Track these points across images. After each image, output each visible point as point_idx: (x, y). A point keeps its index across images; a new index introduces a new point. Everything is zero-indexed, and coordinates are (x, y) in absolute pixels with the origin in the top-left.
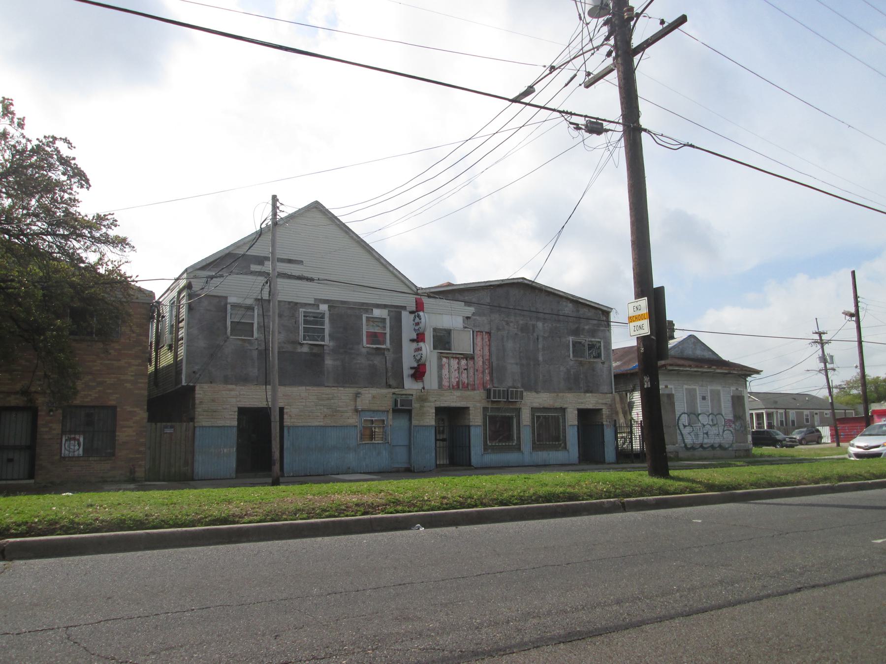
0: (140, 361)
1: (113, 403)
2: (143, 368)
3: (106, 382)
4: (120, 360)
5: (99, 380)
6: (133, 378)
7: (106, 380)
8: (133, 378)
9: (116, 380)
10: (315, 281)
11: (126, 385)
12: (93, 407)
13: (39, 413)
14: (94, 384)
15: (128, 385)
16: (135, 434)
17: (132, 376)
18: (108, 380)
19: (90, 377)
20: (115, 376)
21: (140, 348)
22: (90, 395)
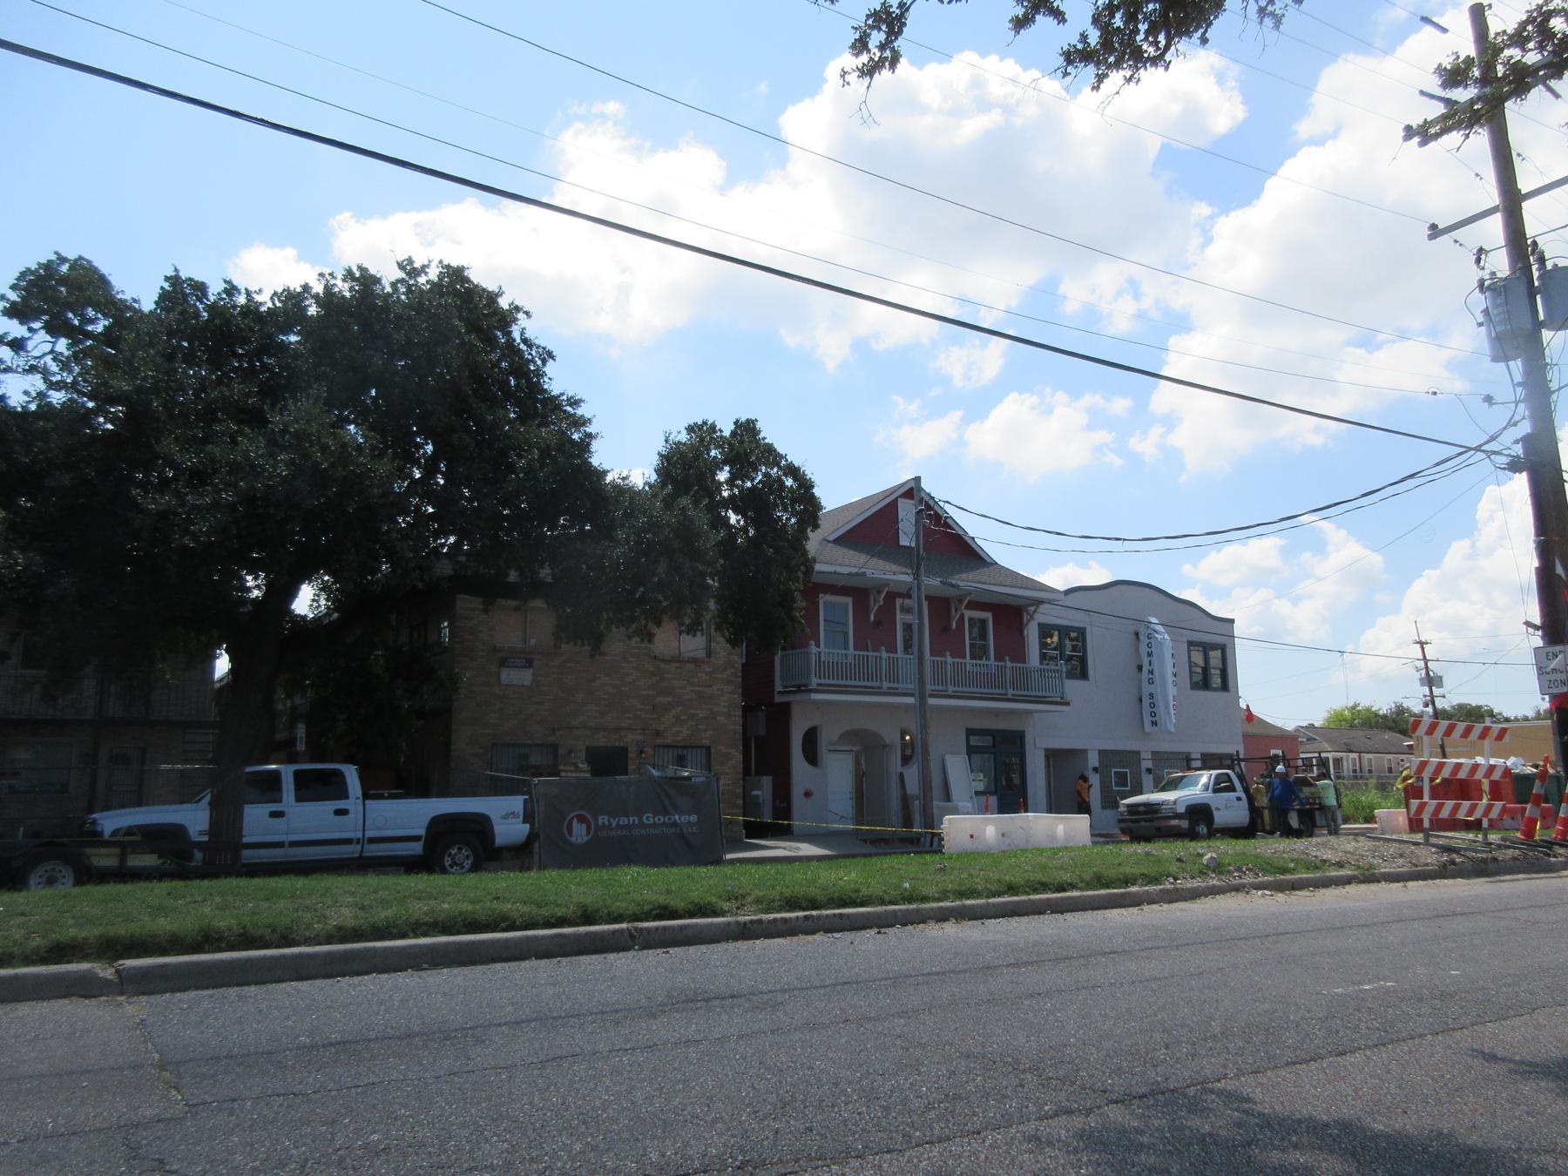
1: (705, 742)
6: (726, 710)
7: (699, 712)
8: (726, 710)
12: (687, 747)
15: (721, 719)
16: (730, 782)
17: (725, 707)
18: (699, 712)
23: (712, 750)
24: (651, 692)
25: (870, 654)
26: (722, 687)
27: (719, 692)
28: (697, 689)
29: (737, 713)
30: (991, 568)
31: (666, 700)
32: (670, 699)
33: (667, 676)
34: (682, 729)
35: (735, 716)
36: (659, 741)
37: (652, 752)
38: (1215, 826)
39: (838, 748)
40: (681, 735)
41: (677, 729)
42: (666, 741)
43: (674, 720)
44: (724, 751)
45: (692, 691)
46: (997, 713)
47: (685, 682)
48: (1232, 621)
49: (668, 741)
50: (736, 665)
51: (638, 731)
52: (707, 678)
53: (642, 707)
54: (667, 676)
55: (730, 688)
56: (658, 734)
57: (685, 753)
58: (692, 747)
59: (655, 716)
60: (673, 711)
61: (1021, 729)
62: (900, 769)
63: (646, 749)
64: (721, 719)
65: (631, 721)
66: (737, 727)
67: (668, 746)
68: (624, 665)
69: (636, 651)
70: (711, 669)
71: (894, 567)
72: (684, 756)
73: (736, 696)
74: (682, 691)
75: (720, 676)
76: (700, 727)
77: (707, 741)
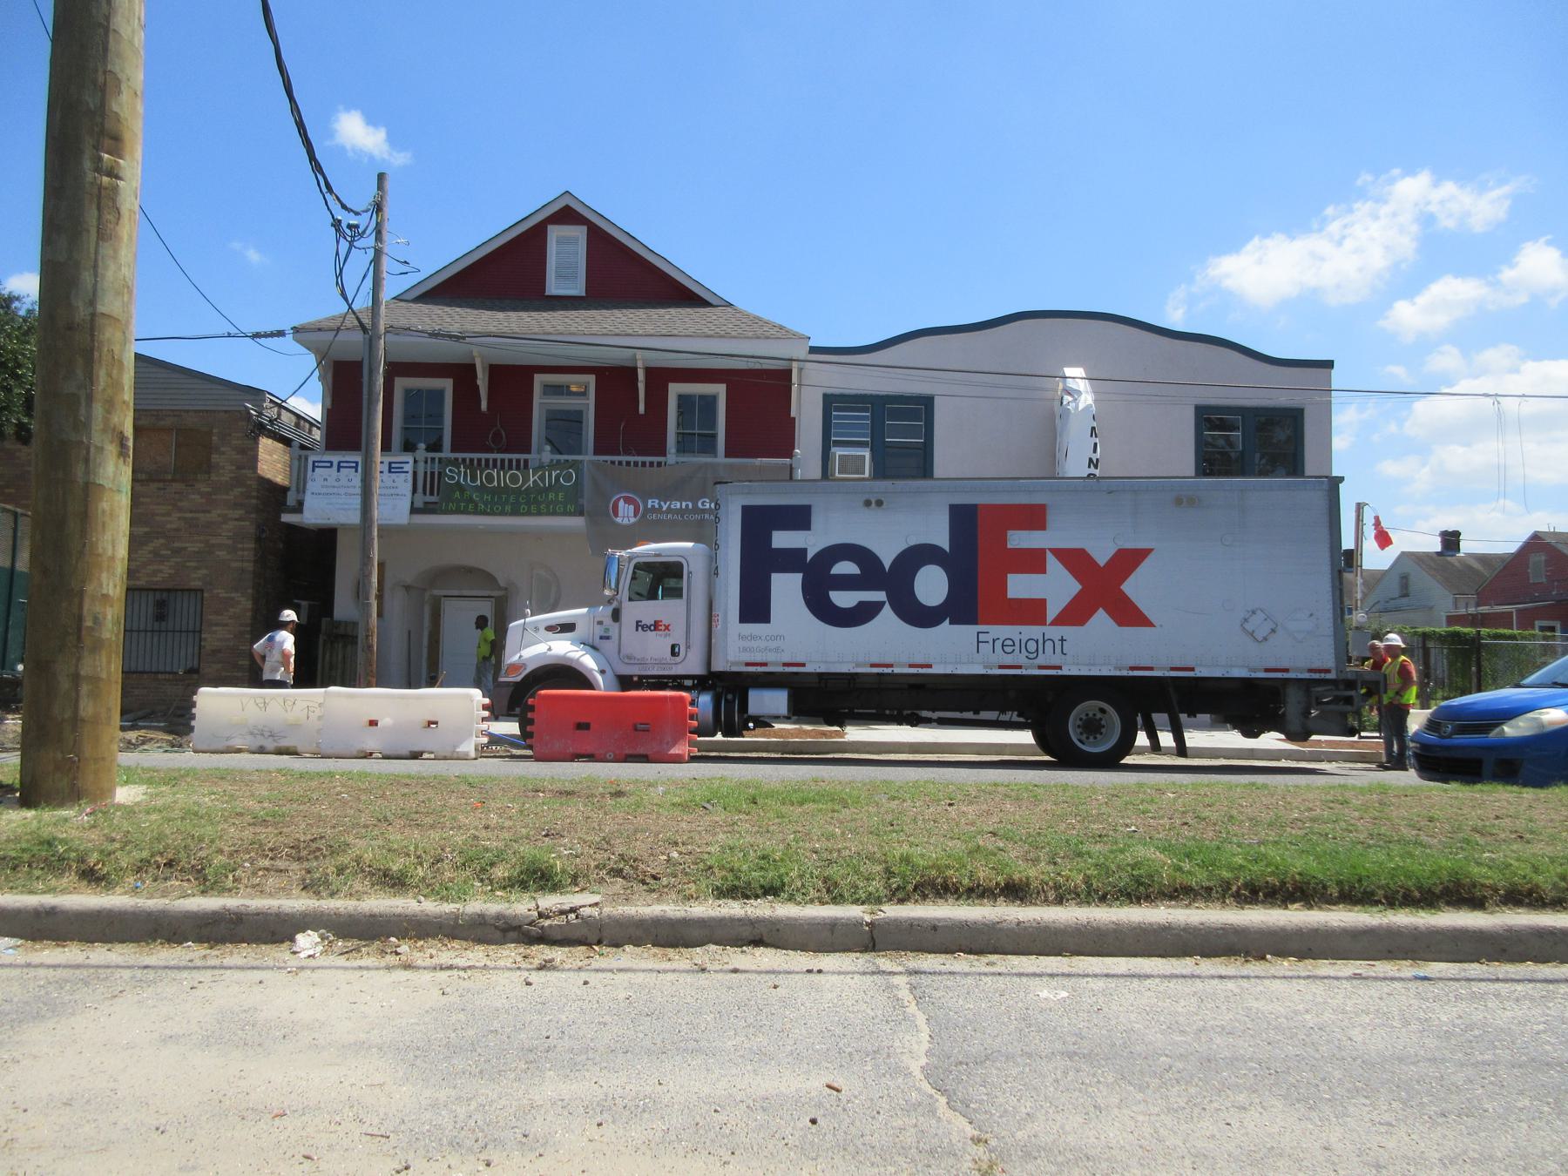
3: (185, 548)
4: (209, 512)
5: (177, 545)
6: (230, 542)
7: (184, 545)
8: (230, 542)
9: (203, 545)
11: (217, 553)
12: (169, 590)
15: (222, 554)
18: (187, 545)
19: (162, 541)
20: (202, 538)
22: (161, 571)
23: (205, 595)
26: (226, 512)
27: (220, 519)
28: (189, 515)
29: (246, 546)
32: (146, 529)
33: (141, 499)
34: (162, 567)
35: (243, 549)
41: (156, 567)
42: (138, 583)
43: (151, 556)
45: (179, 518)
47: (170, 507)
48: (1329, 364)
50: (249, 482)
52: (204, 500)
54: (141, 499)
55: (239, 513)
60: (151, 544)
64: (222, 554)
66: (246, 564)
72: (164, 601)
73: (248, 523)
74: (164, 519)
75: (225, 497)
76: (188, 564)
77: (200, 583)
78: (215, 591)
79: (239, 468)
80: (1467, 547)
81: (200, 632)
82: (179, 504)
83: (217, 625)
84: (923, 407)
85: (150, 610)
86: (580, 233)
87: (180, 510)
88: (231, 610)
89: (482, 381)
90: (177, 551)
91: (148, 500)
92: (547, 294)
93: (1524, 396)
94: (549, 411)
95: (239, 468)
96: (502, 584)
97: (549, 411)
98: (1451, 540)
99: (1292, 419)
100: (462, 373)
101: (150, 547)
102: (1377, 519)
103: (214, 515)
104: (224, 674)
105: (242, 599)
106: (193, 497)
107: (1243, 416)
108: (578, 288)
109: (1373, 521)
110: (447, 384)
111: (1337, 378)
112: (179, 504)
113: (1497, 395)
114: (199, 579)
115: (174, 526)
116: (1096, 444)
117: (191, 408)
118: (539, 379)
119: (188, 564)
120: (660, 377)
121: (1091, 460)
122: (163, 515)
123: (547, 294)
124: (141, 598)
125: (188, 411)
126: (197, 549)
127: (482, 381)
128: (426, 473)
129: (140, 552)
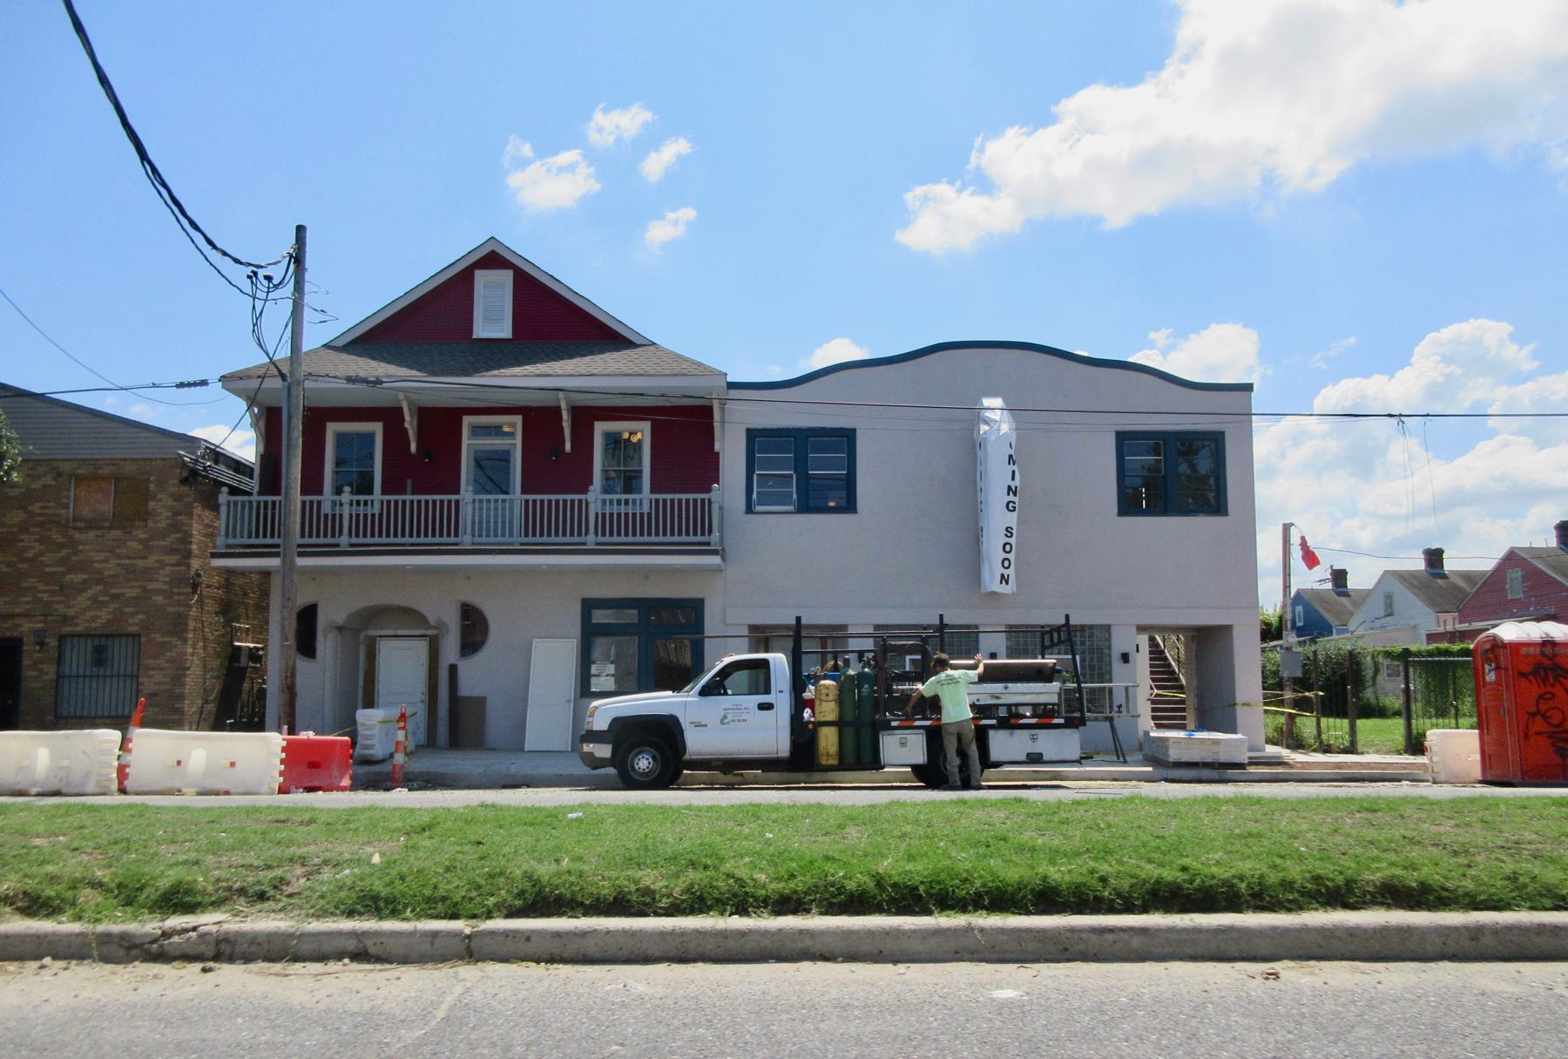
0: (178, 557)
1: (134, 629)
2: (183, 568)
3: (123, 594)
4: (146, 558)
5: (114, 591)
6: (167, 587)
7: (123, 591)
8: (167, 587)
10: (385, 385)
12: (108, 636)
13: (25, 648)
14: (106, 599)
15: (159, 599)
17: (165, 583)
19: (99, 588)
20: (139, 583)
21: (179, 536)
23: (142, 639)
24: (60, 569)
25: (408, 497)
27: (157, 565)
28: (127, 562)
29: (182, 590)
30: (638, 350)
31: (79, 577)
32: (84, 576)
33: (81, 547)
36: (67, 629)
37: (57, 644)
38: (687, 757)
39: (400, 632)
40: (99, 621)
41: (94, 614)
43: (89, 603)
44: (158, 640)
45: (118, 565)
46: (647, 573)
47: (109, 554)
48: (1248, 388)
49: (80, 629)
51: (39, 618)
52: (141, 547)
53: (44, 588)
56: (65, 619)
57: (103, 642)
58: (121, 636)
59: (62, 599)
61: (700, 596)
62: (453, 661)
63: (47, 640)
64: (159, 599)
65: (28, 606)
67: (79, 636)
68: (23, 537)
69: (41, 519)
70: (147, 536)
71: (414, 372)
74: (103, 565)
75: (162, 543)
76: (126, 610)
78: (152, 636)
79: (176, 514)
80: (1449, 565)
81: (138, 677)
82: (118, 551)
83: (155, 669)
84: (846, 437)
85: (89, 657)
86: (507, 277)
87: (118, 557)
88: (168, 654)
89: (410, 423)
90: (115, 597)
91: (87, 547)
92: (474, 336)
93: (1428, 415)
94: (476, 452)
95: (176, 514)
96: (432, 623)
97: (476, 452)
98: (1434, 558)
99: (1216, 441)
100: (390, 416)
101: (90, 593)
102: (1303, 539)
103: (151, 561)
104: (160, 717)
105: (179, 643)
106: (130, 543)
107: (1164, 440)
108: (504, 331)
109: (1300, 541)
110: (377, 428)
111: (1257, 401)
112: (118, 551)
113: (1401, 415)
114: (136, 624)
115: (112, 573)
116: (1014, 472)
117: (127, 457)
118: (467, 421)
119: (126, 610)
120: (586, 416)
121: (1009, 488)
122: (98, 562)
123: (474, 336)
124: (86, 644)
125: (125, 460)
126: (133, 595)
127: (410, 423)
128: (351, 515)
129: (79, 598)
